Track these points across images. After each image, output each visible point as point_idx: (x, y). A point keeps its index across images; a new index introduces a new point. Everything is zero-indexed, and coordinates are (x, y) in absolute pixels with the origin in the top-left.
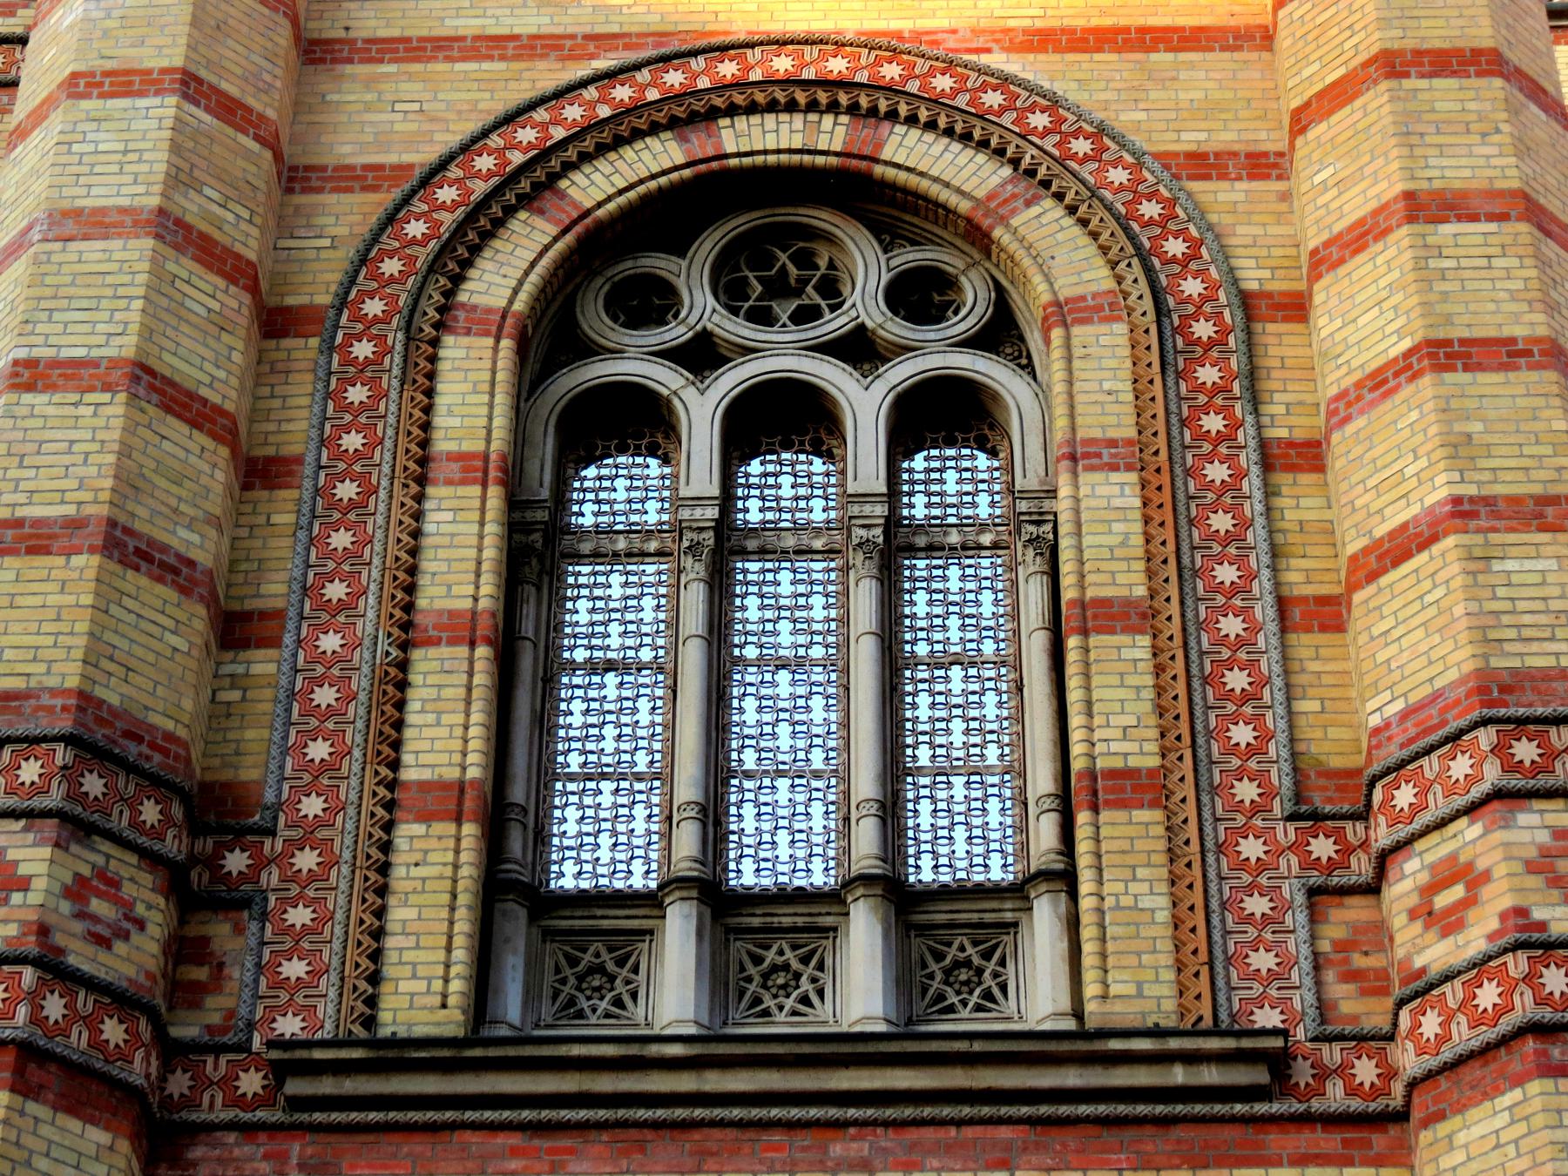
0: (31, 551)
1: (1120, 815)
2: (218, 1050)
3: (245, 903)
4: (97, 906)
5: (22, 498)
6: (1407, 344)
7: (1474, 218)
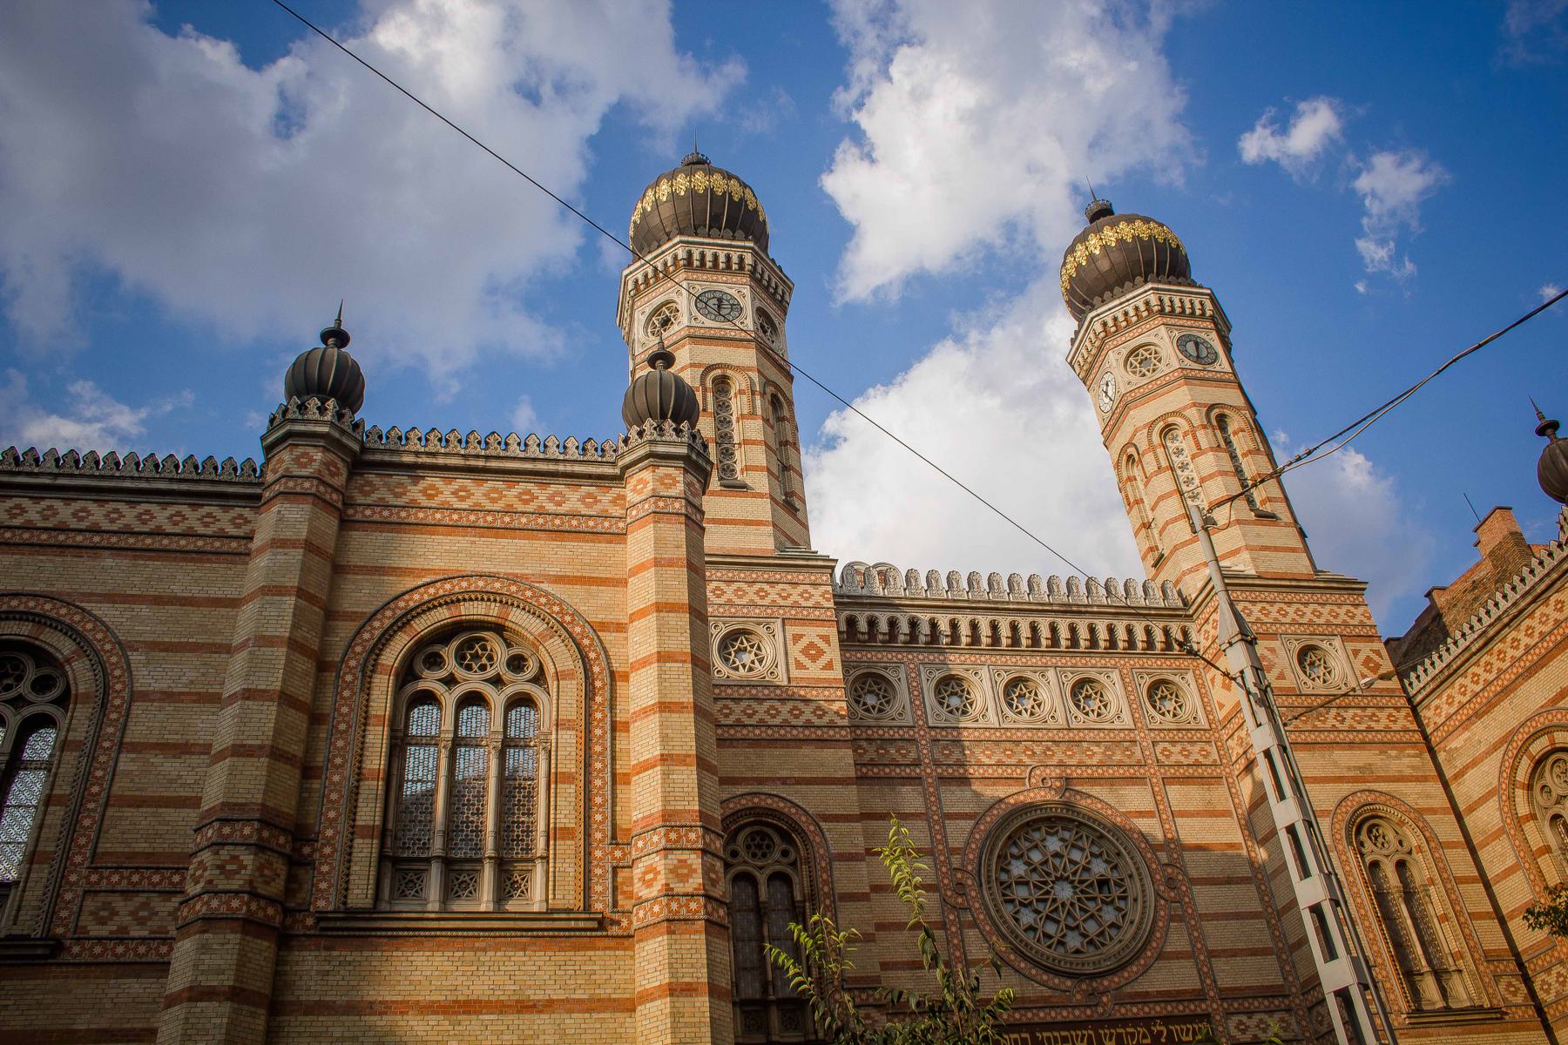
0: (248, 756)
1: (562, 842)
2: (300, 911)
3: (308, 864)
4: (266, 872)
5: (245, 737)
6: (653, 702)
7: (676, 661)
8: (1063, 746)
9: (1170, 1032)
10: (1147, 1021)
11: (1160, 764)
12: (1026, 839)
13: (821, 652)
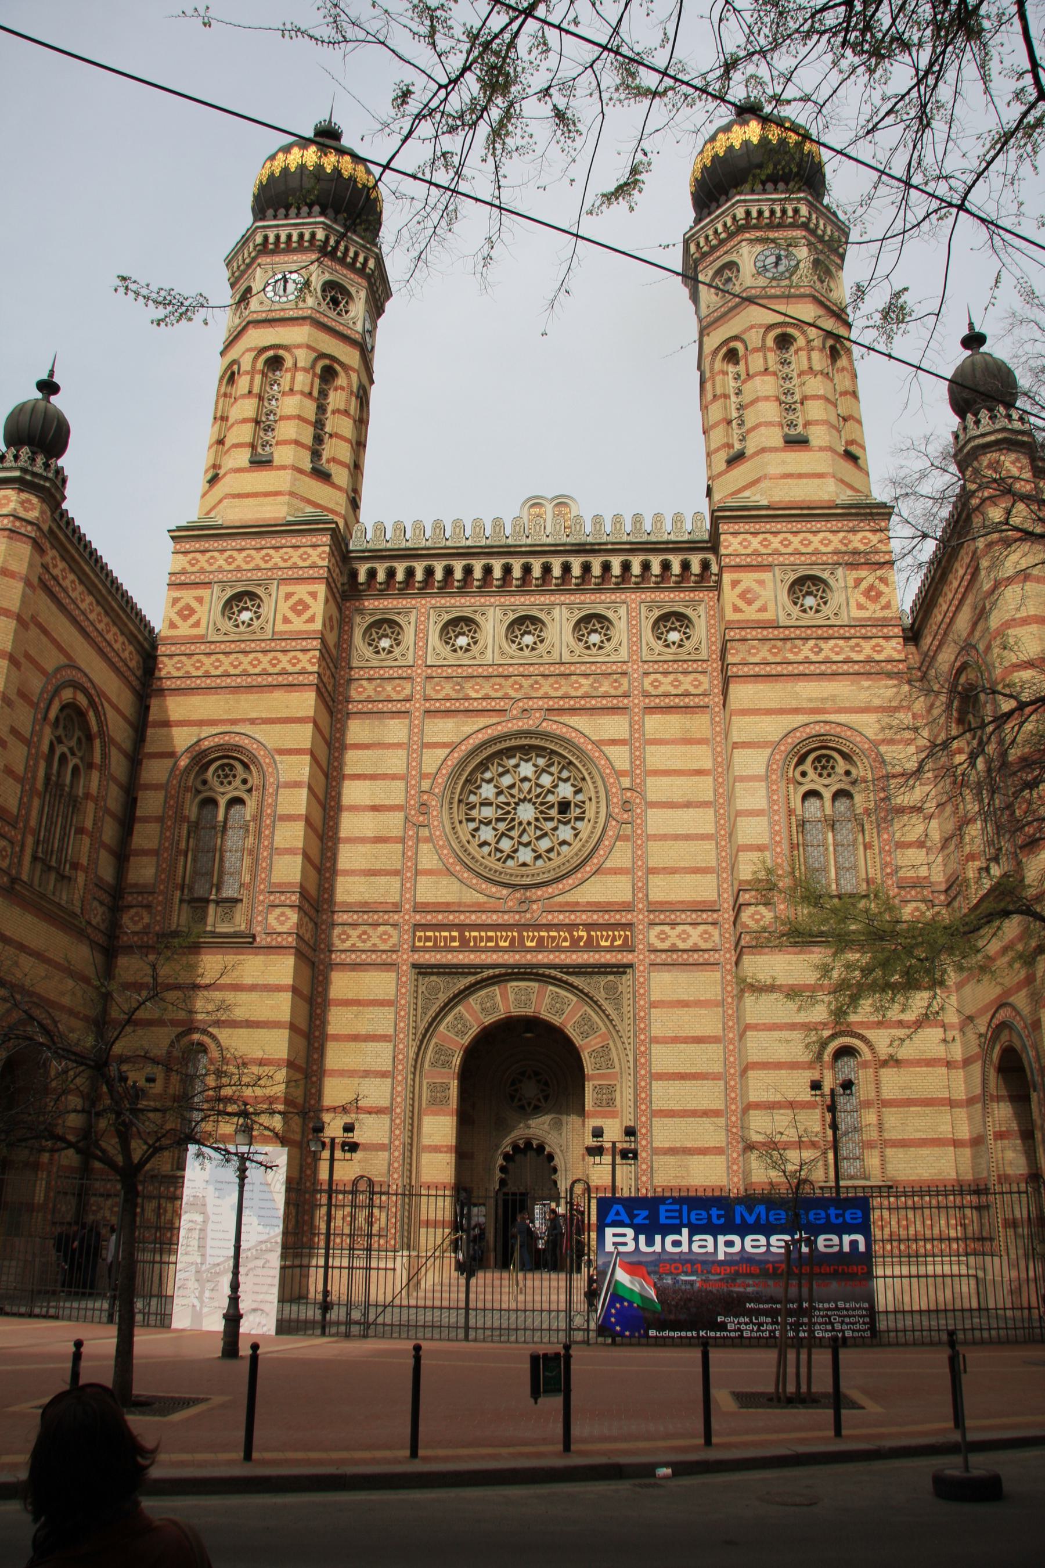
8: (552, 680)
9: (590, 937)
10: (572, 927)
11: (646, 695)
12: (499, 765)
13: (307, 607)
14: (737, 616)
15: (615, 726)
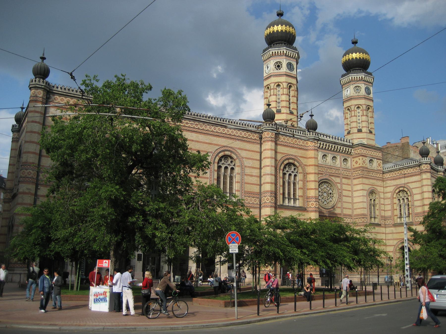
14: (363, 166)
15: (338, 180)
